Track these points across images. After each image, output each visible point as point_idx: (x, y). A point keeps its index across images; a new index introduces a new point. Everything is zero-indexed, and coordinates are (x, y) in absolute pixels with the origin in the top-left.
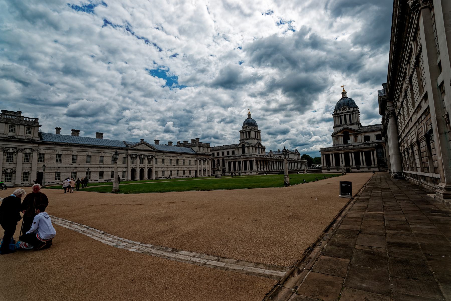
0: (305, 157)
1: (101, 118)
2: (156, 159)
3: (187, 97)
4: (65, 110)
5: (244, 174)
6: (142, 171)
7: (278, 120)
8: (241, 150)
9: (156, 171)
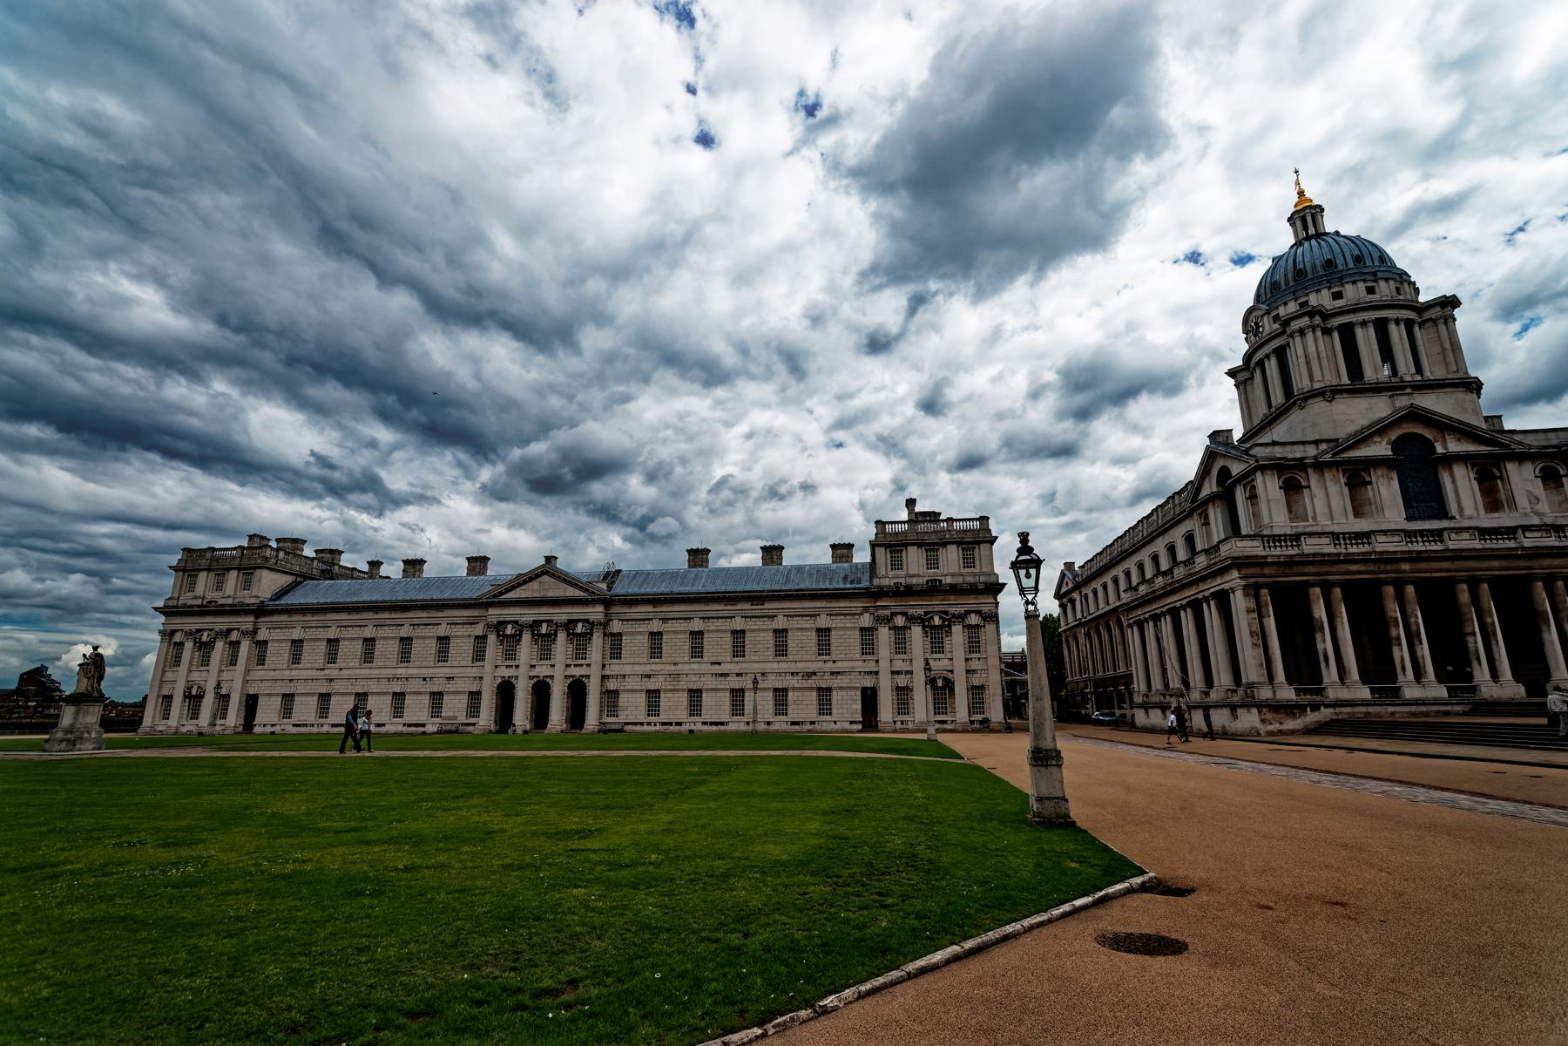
6: (541, 690)
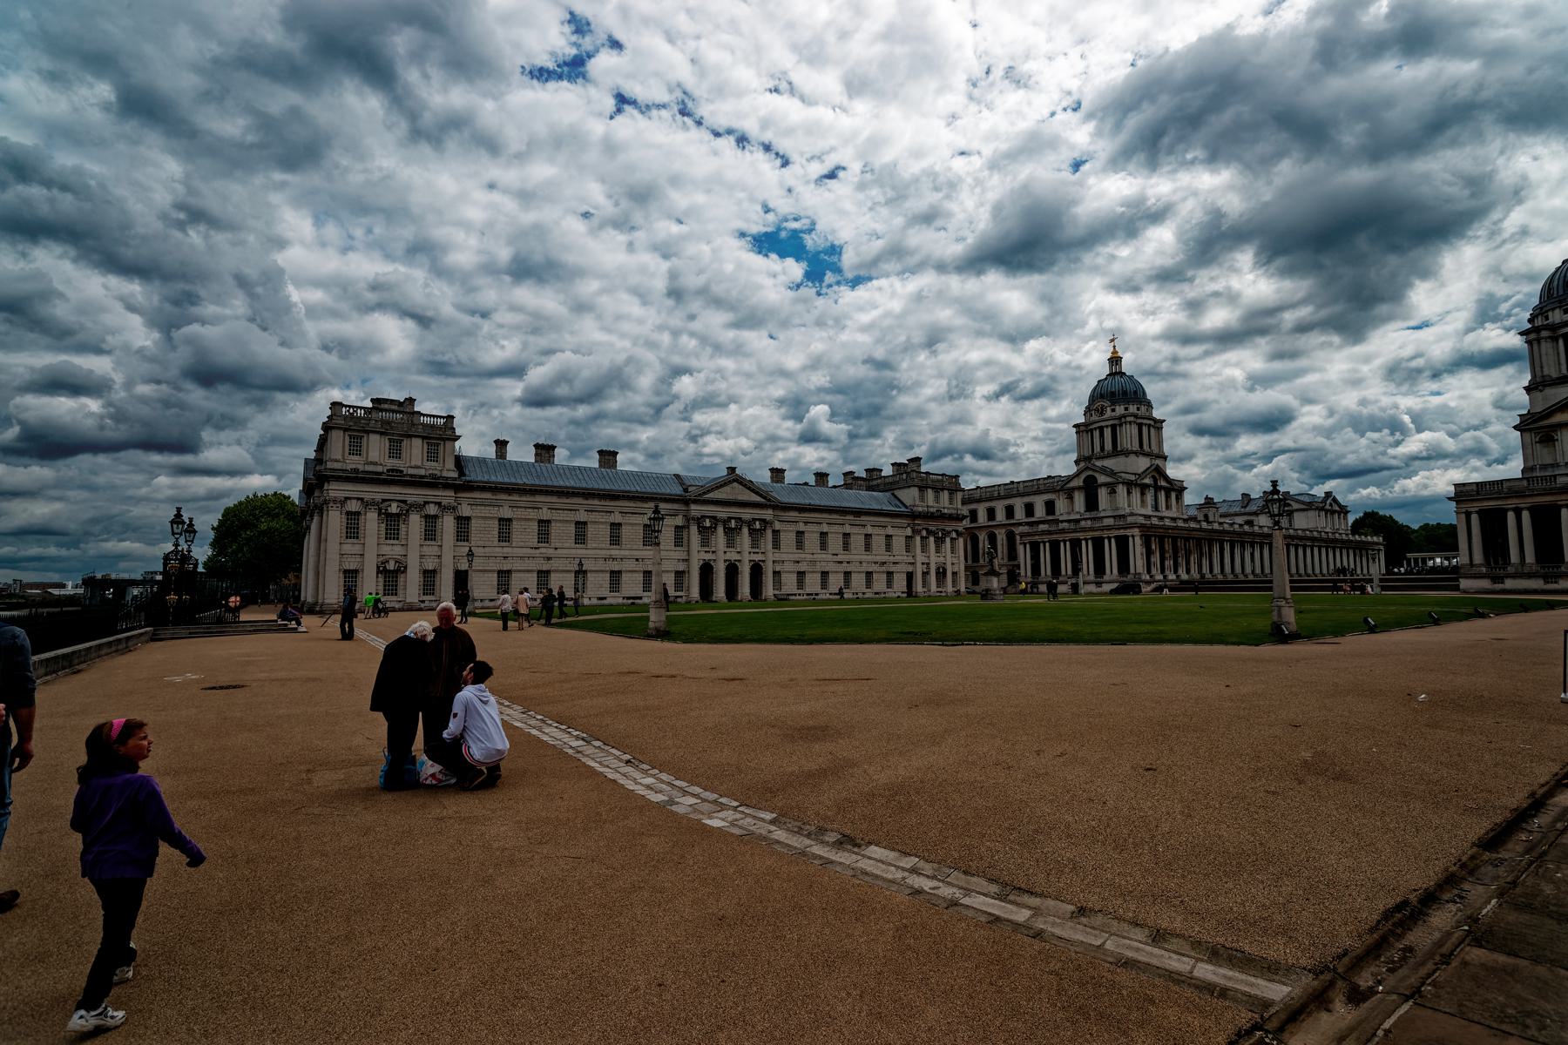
0: (1373, 521)
1: (612, 405)
2: (776, 533)
3: (875, 314)
4: (516, 388)
5: (1092, 588)
6: (732, 570)
7: (1238, 374)
8: (1079, 500)
9: (776, 574)
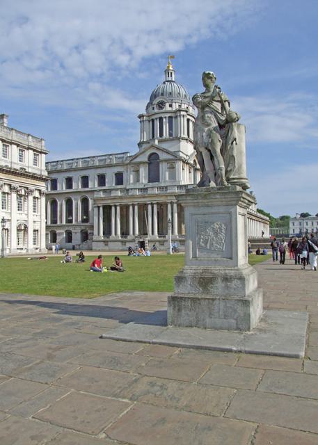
8: (143, 172)
